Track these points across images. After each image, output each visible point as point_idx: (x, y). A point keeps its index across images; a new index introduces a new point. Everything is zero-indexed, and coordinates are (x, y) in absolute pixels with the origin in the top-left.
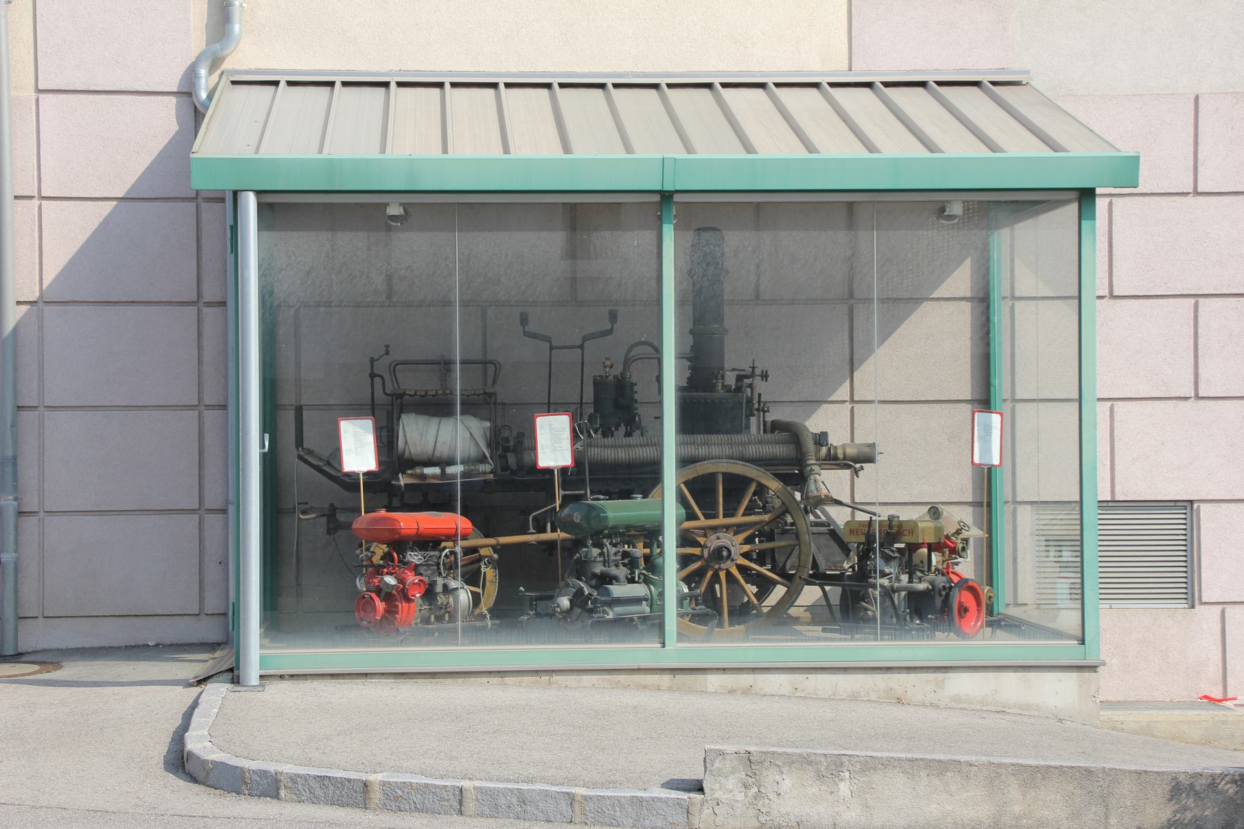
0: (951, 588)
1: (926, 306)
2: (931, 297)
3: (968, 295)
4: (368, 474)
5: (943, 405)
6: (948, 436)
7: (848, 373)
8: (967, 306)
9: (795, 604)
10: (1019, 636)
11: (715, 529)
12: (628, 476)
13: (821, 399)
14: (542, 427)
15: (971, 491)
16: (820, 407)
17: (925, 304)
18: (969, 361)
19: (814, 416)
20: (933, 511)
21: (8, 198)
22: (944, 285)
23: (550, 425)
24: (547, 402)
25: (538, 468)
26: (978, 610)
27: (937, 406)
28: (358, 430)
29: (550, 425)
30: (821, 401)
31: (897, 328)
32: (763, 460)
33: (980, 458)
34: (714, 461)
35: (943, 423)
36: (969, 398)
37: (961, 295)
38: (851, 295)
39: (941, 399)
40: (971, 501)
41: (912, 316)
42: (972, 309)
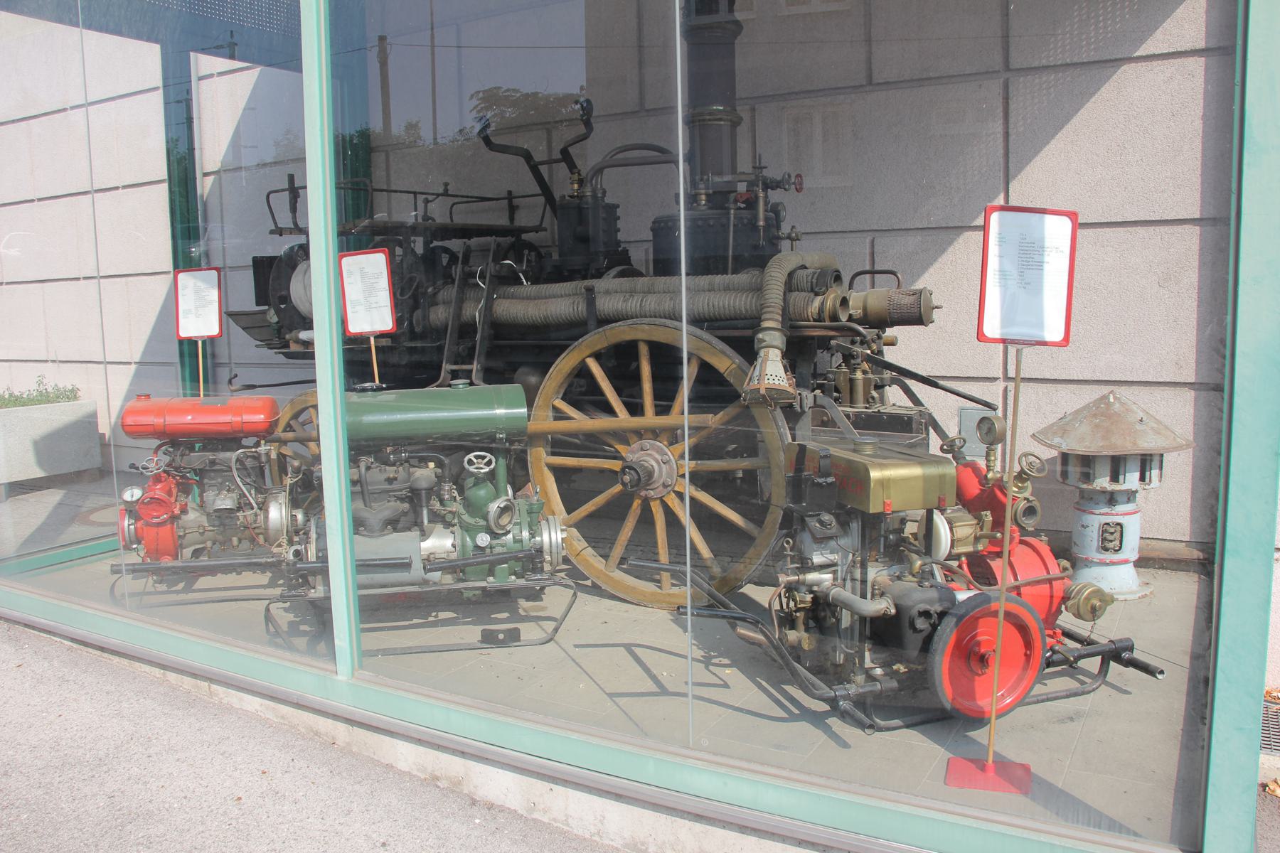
0: (942, 615)
1: (1127, 72)
2: (1138, 54)
3: (1201, 44)
4: (380, 336)
5: (1151, 229)
6: (1159, 277)
7: (1002, 186)
8: (1197, 66)
9: (540, 623)
10: (1057, 814)
11: (639, 433)
12: (419, 344)
13: (960, 224)
14: (351, 273)
15: (1194, 365)
16: (958, 236)
17: (1125, 67)
18: (1199, 155)
19: (951, 249)
20: (985, 427)
21: (194, 78)
22: (1159, 34)
23: (362, 269)
24: (877, 268)
25: (395, 329)
26: (1026, 655)
27: (1141, 231)
28: (200, 284)
29: (362, 269)
30: (961, 227)
31: (1079, 110)
32: (721, 320)
33: (1006, 320)
34: (629, 322)
35: (1151, 258)
36: (1197, 216)
37: (1187, 46)
38: (1007, 67)
39: (1148, 219)
40: (1193, 381)
41: (1103, 89)
42: (1206, 70)
